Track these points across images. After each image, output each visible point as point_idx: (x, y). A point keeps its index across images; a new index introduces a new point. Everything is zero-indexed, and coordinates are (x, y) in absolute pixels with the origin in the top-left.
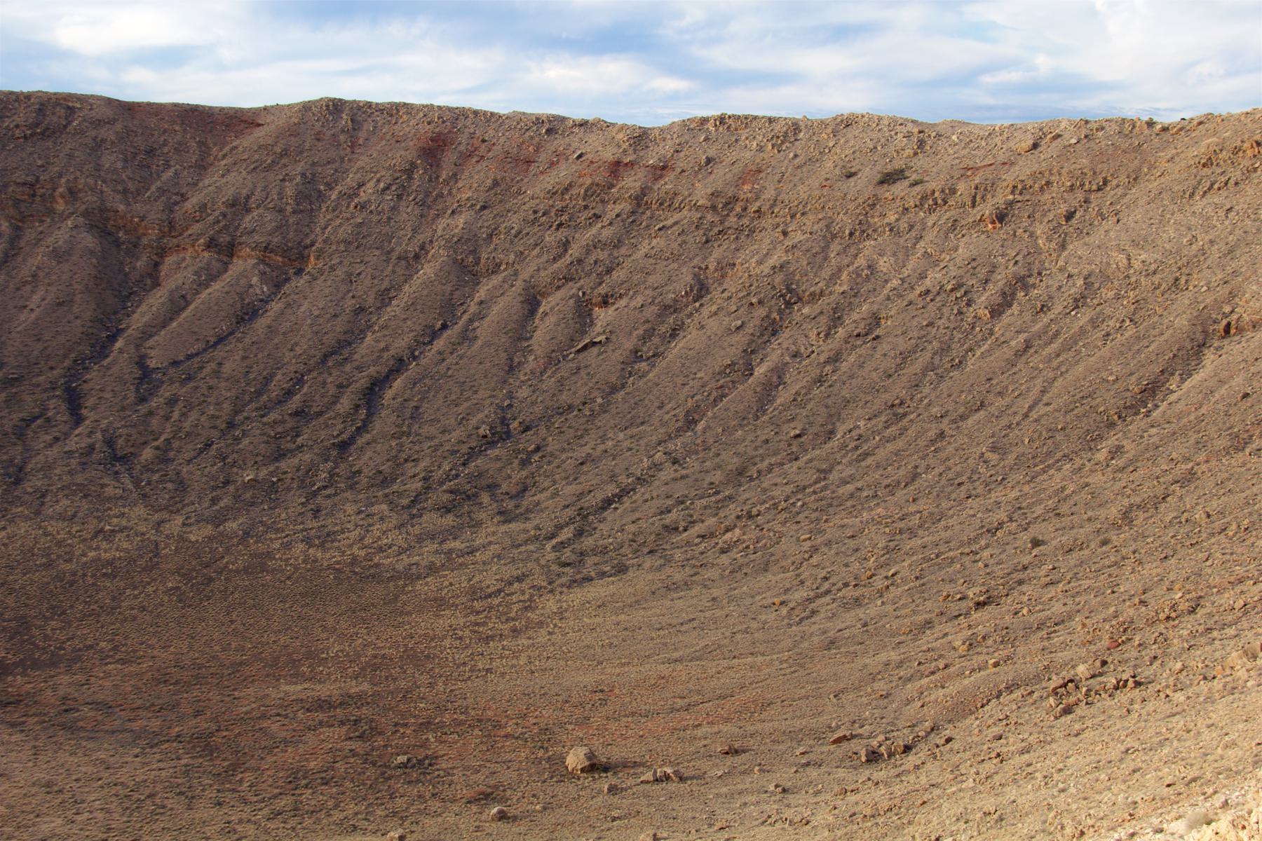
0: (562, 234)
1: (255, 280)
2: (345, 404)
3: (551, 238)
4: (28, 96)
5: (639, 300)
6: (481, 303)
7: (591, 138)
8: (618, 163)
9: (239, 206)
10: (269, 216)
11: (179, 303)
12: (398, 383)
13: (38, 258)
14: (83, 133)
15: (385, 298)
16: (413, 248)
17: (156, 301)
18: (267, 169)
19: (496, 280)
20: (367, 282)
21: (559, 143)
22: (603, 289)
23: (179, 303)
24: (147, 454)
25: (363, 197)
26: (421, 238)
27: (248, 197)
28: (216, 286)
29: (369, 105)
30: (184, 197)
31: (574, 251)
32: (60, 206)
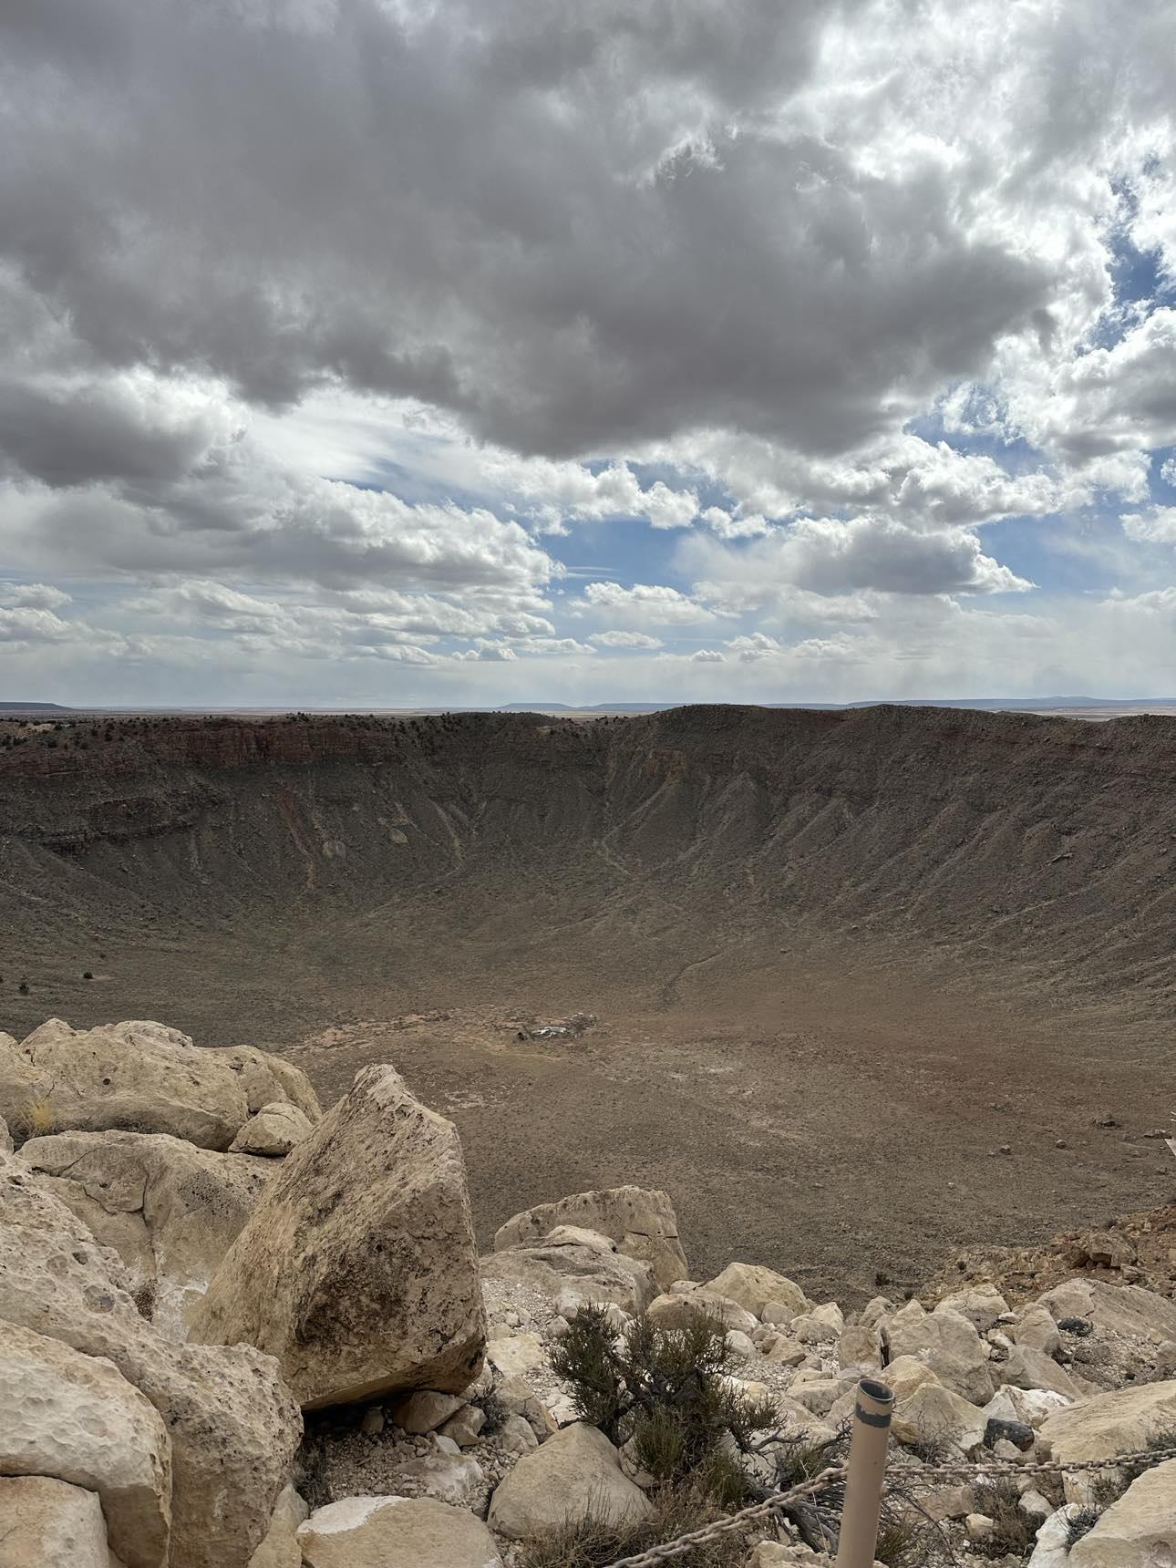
0: (1039, 789)
3: (1030, 790)
5: (1093, 832)
7: (1055, 729)
8: (1073, 745)
9: (835, 768)
11: (801, 824)
12: (937, 873)
13: (724, 797)
15: (925, 823)
17: (790, 820)
19: (994, 816)
21: (1033, 732)
22: (1068, 824)
23: (801, 824)
28: (823, 813)
31: (1047, 799)
32: (736, 766)
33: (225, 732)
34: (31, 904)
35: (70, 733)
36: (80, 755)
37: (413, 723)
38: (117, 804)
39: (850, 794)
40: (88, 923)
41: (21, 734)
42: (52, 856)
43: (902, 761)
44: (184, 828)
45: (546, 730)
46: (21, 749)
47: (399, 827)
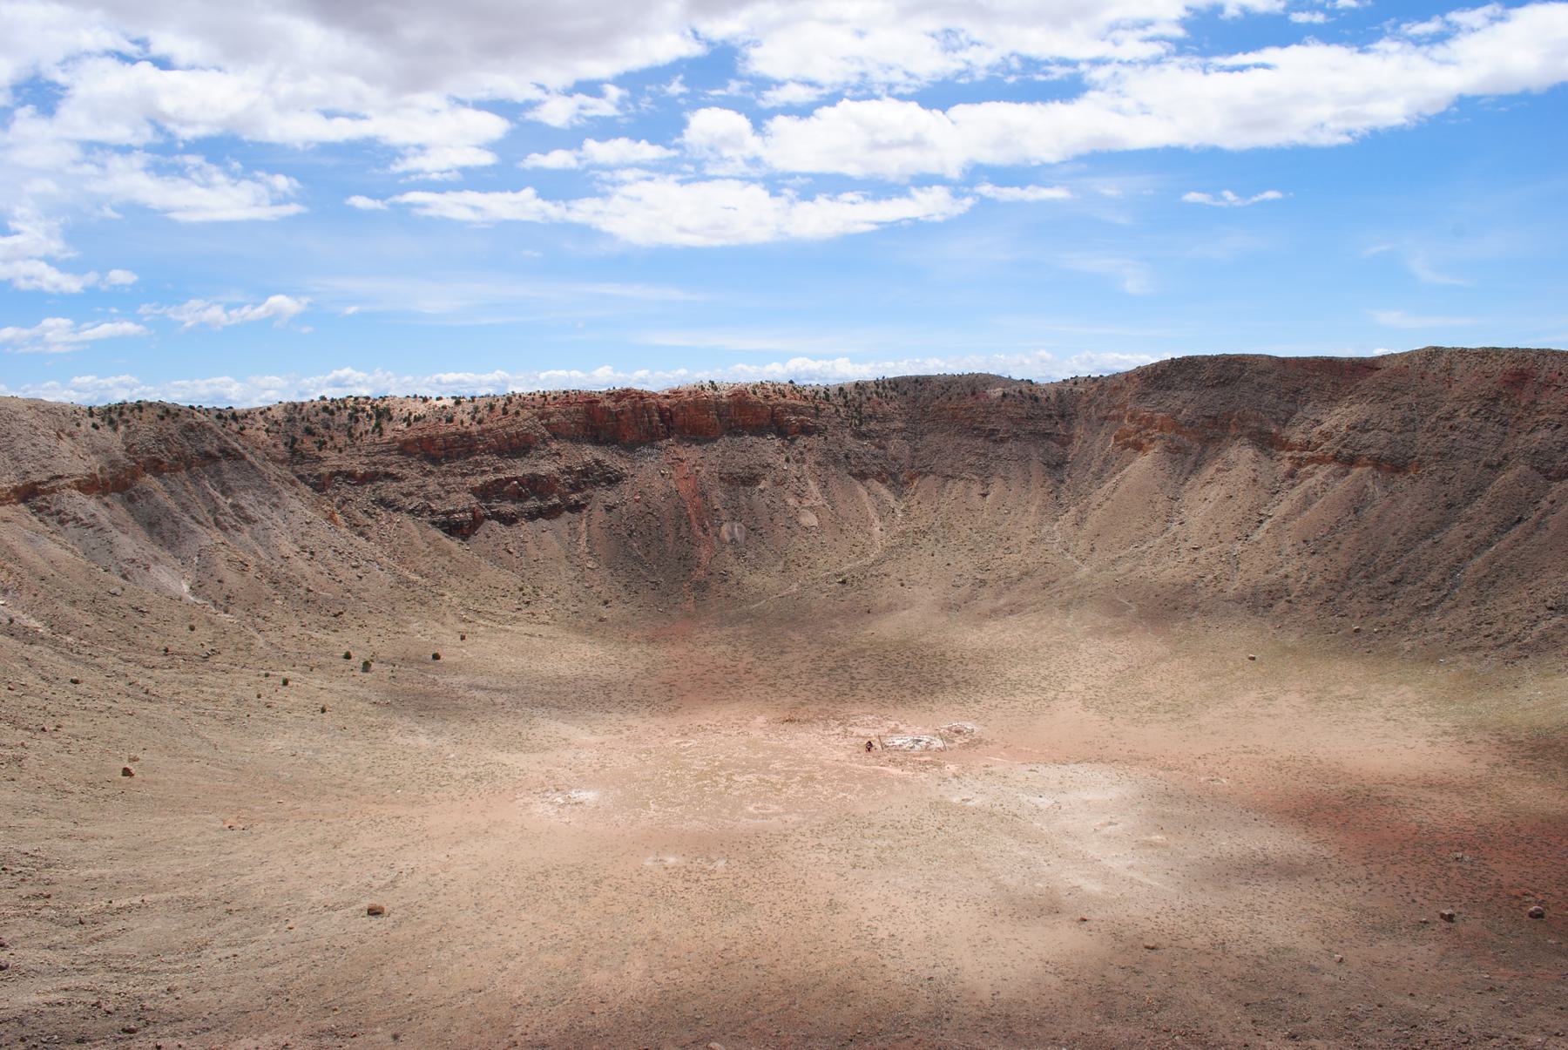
1: (1370, 483)
2: (1434, 577)
4: (1217, 358)
6: (1552, 502)
10: (1383, 434)
12: (1478, 560)
14: (1247, 380)
15: (1472, 494)
16: (1496, 459)
17: (1296, 493)
18: (1382, 401)
20: (1458, 485)
24: (1281, 605)
25: (1455, 422)
26: (1505, 450)
27: (1367, 421)
29: (1463, 351)
30: (1319, 422)
33: (626, 402)
34: (409, 583)
35: (470, 407)
36: (475, 428)
37: (841, 389)
38: (508, 480)
39: (1377, 463)
40: (461, 604)
41: (421, 409)
42: (439, 534)
43: (1451, 415)
44: (576, 508)
45: (998, 392)
46: (420, 424)
47: (811, 508)
